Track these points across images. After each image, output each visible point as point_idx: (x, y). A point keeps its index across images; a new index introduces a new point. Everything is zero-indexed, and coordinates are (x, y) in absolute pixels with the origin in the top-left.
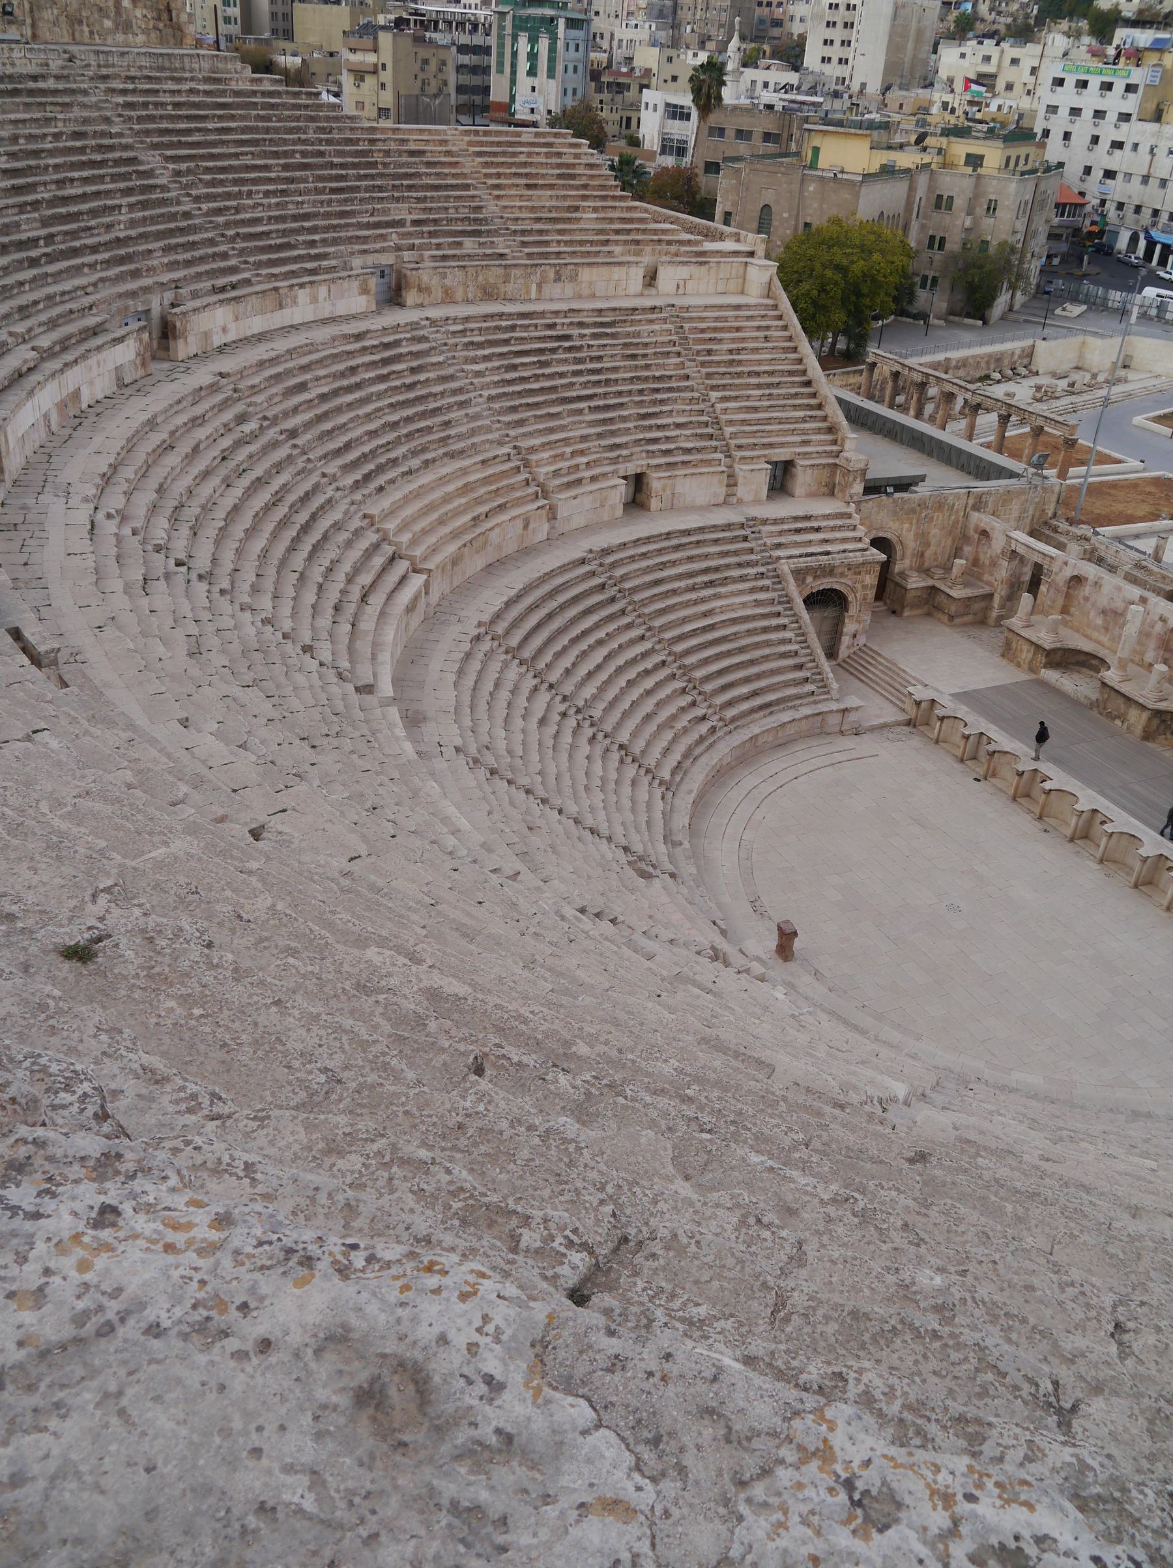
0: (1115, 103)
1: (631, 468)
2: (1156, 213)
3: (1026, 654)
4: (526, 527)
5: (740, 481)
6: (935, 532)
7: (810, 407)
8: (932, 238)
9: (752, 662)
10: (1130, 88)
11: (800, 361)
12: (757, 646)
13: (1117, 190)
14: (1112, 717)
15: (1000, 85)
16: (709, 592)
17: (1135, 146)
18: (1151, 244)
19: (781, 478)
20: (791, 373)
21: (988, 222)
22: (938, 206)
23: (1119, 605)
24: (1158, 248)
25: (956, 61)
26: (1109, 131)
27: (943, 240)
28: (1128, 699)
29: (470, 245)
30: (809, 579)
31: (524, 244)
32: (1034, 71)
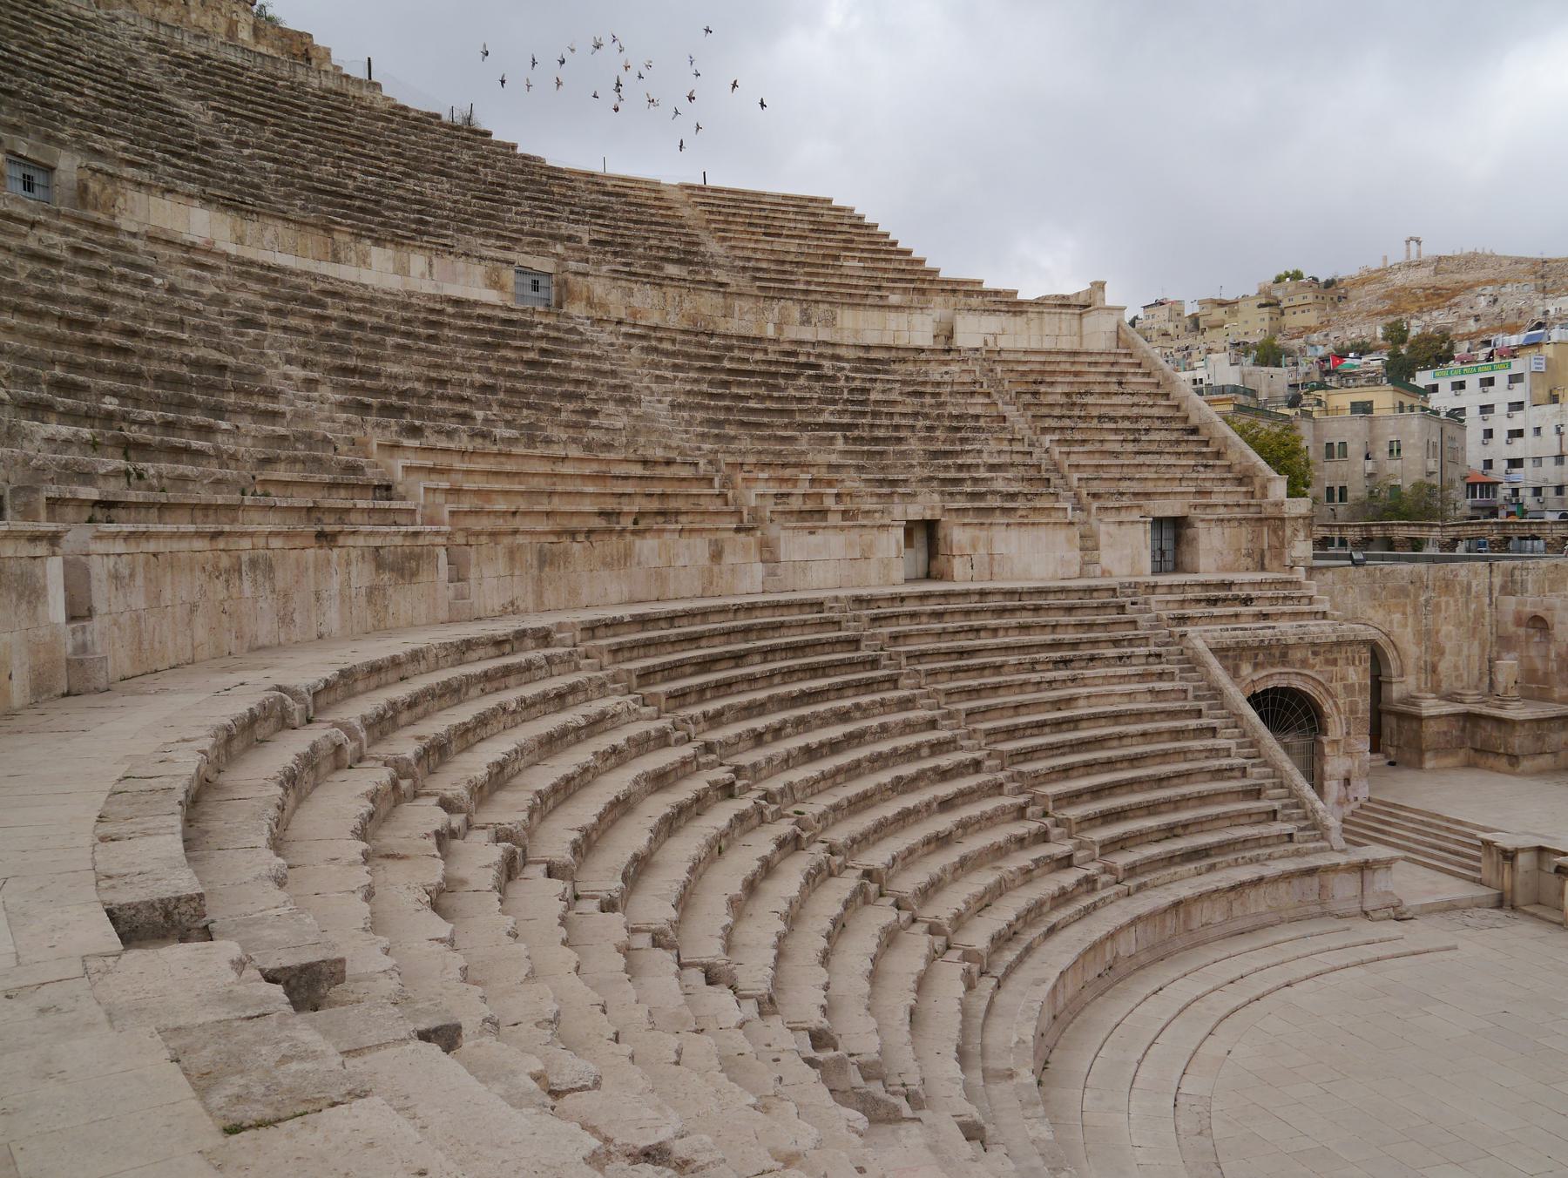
1: (916, 512)
4: (717, 556)
5: (1103, 539)
6: (1448, 631)
8: (1330, 490)
9: (1160, 781)
11: (1178, 407)
12: (1165, 756)
13: (1526, 477)
16: (1063, 674)
17: (1538, 430)
19: (1173, 536)
21: (1393, 466)
26: (1501, 423)
27: (1343, 490)
29: (672, 270)
30: (1246, 669)
31: (755, 279)
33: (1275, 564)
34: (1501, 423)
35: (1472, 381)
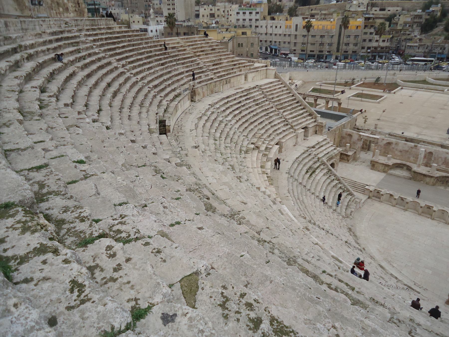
0: (254, 17)
2: (271, 42)
3: (381, 168)
7: (302, 109)
10: (257, 13)
14: (419, 181)
15: (216, 16)
17: (261, 27)
18: (271, 50)
20: (293, 100)
22: (239, 46)
23: (406, 148)
24: (274, 50)
25: (204, 11)
28: (425, 175)
32: (224, 11)
33: (320, 133)
34: (254, 24)
35: (247, 12)
